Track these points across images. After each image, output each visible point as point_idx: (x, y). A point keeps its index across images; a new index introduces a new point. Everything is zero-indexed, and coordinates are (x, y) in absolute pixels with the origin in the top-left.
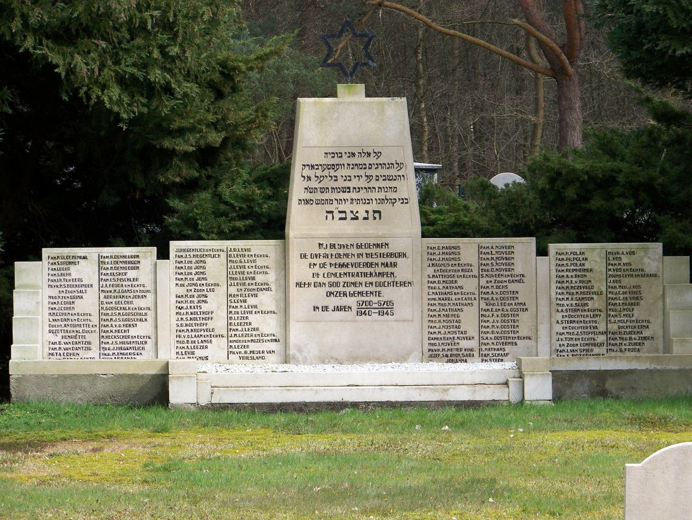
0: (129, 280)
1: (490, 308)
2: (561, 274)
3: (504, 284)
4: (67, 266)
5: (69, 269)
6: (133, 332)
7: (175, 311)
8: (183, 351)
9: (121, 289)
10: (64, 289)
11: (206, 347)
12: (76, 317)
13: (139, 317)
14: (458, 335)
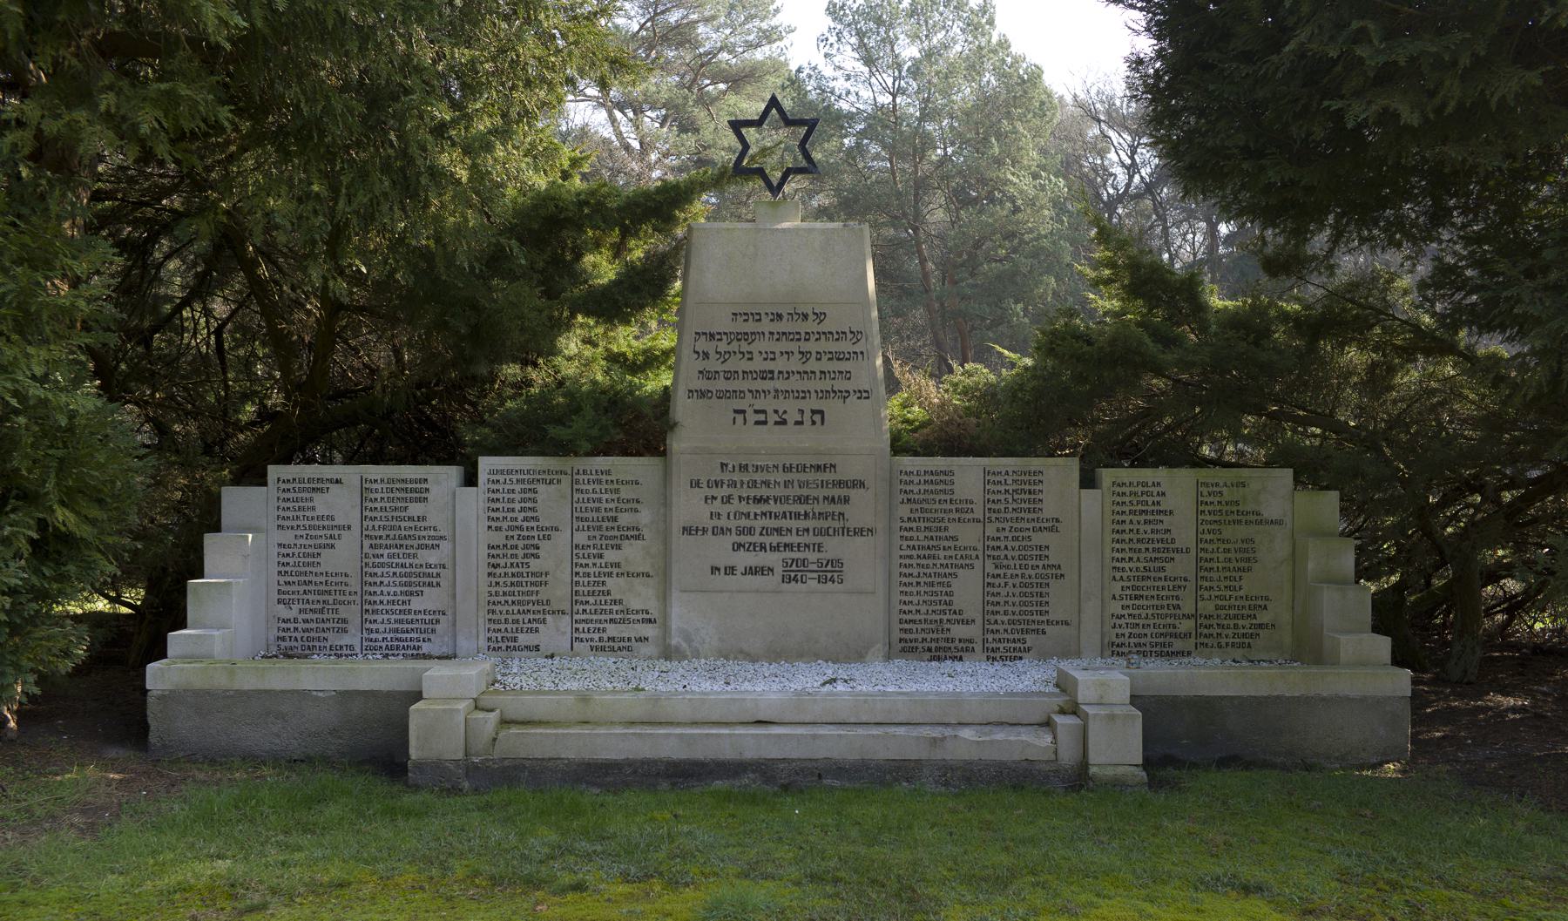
0: (411, 519)
1: (1001, 572)
2: (1121, 518)
3: (1025, 534)
4: (308, 495)
5: (311, 500)
6: (416, 604)
7: (485, 570)
8: (499, 635)
9: (398, 533)
10: (304, 533)
11: (537, 630)
12: (323, 579)
13: (427, 580)
14: (948, 616)
